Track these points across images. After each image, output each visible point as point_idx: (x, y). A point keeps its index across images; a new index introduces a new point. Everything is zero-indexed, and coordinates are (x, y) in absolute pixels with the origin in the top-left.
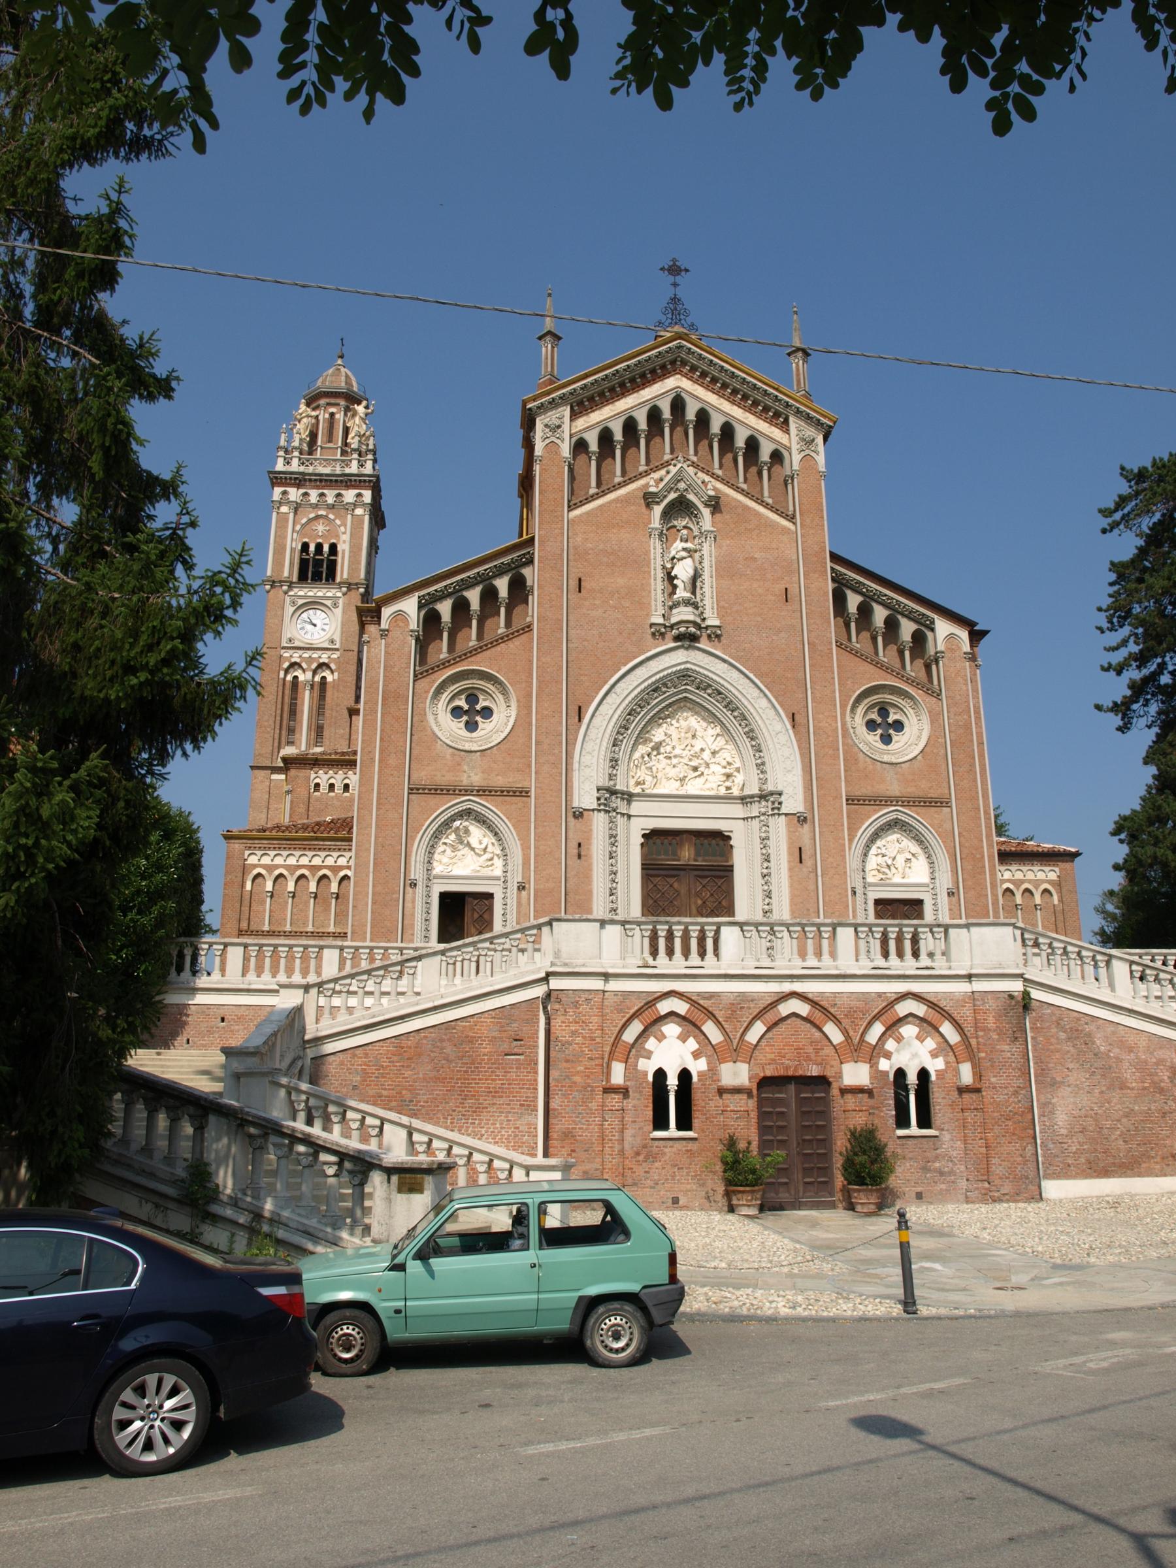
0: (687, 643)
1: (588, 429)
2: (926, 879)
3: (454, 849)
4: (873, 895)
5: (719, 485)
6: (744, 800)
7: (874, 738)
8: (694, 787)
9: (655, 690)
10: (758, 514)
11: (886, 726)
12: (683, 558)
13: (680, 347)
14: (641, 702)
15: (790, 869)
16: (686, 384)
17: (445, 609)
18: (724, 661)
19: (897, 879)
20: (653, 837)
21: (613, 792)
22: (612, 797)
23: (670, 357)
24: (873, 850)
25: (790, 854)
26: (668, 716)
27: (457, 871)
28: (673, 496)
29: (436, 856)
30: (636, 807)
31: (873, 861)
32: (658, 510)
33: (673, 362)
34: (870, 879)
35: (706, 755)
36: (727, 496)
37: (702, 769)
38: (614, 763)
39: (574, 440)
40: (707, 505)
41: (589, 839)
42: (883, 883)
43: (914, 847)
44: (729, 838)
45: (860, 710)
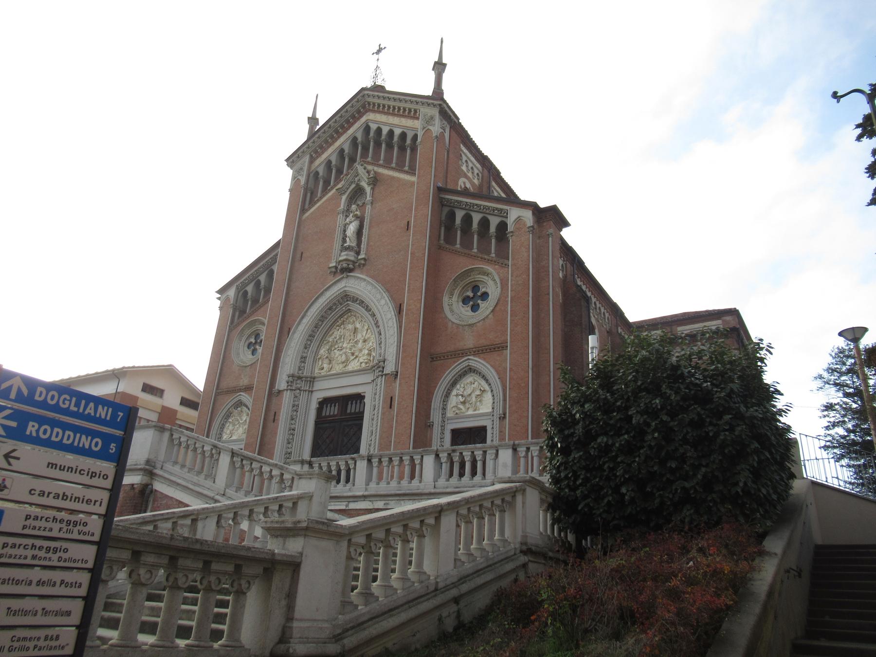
0: (344, 275)
1: (320, 165)
2: (490, 410)
3: (234, 425)
4: (450, 427)
5: (381, 170)
6: (372, 369)
7: (465, 311)
8: (354, 365)
9: (330, 309)
10: (399, 179)
11: (474, 297)
12: (351, 222)
13: (363, 96)
14: (322, 318)
15: (383, 414)
16: (371, 116)
17: (250, 289)
18: (365, 280)
19: (470, 412)
20: (324, 403)
21: (300, 378)
22: (303, 381)
23: (360, 104)
24: (454, 392)
25: (384, 402)
26: (343, 323)
27: (234, 438)
28: (353, 186)
29: (225, 430)
30: (318, 385)
31: (453, 400)
32: (344, 197)
33: (364, 106)
34: (450, 414)
35: (360, 345)
36: (383, 174)
37: (356, 354)
38: (303, 359)
39: (312, 175)
40: (369, 185)
41: (280, 409)
42: (457, 416)
43: (487, 387)
44: (364, 397)
45: (457, 292)
